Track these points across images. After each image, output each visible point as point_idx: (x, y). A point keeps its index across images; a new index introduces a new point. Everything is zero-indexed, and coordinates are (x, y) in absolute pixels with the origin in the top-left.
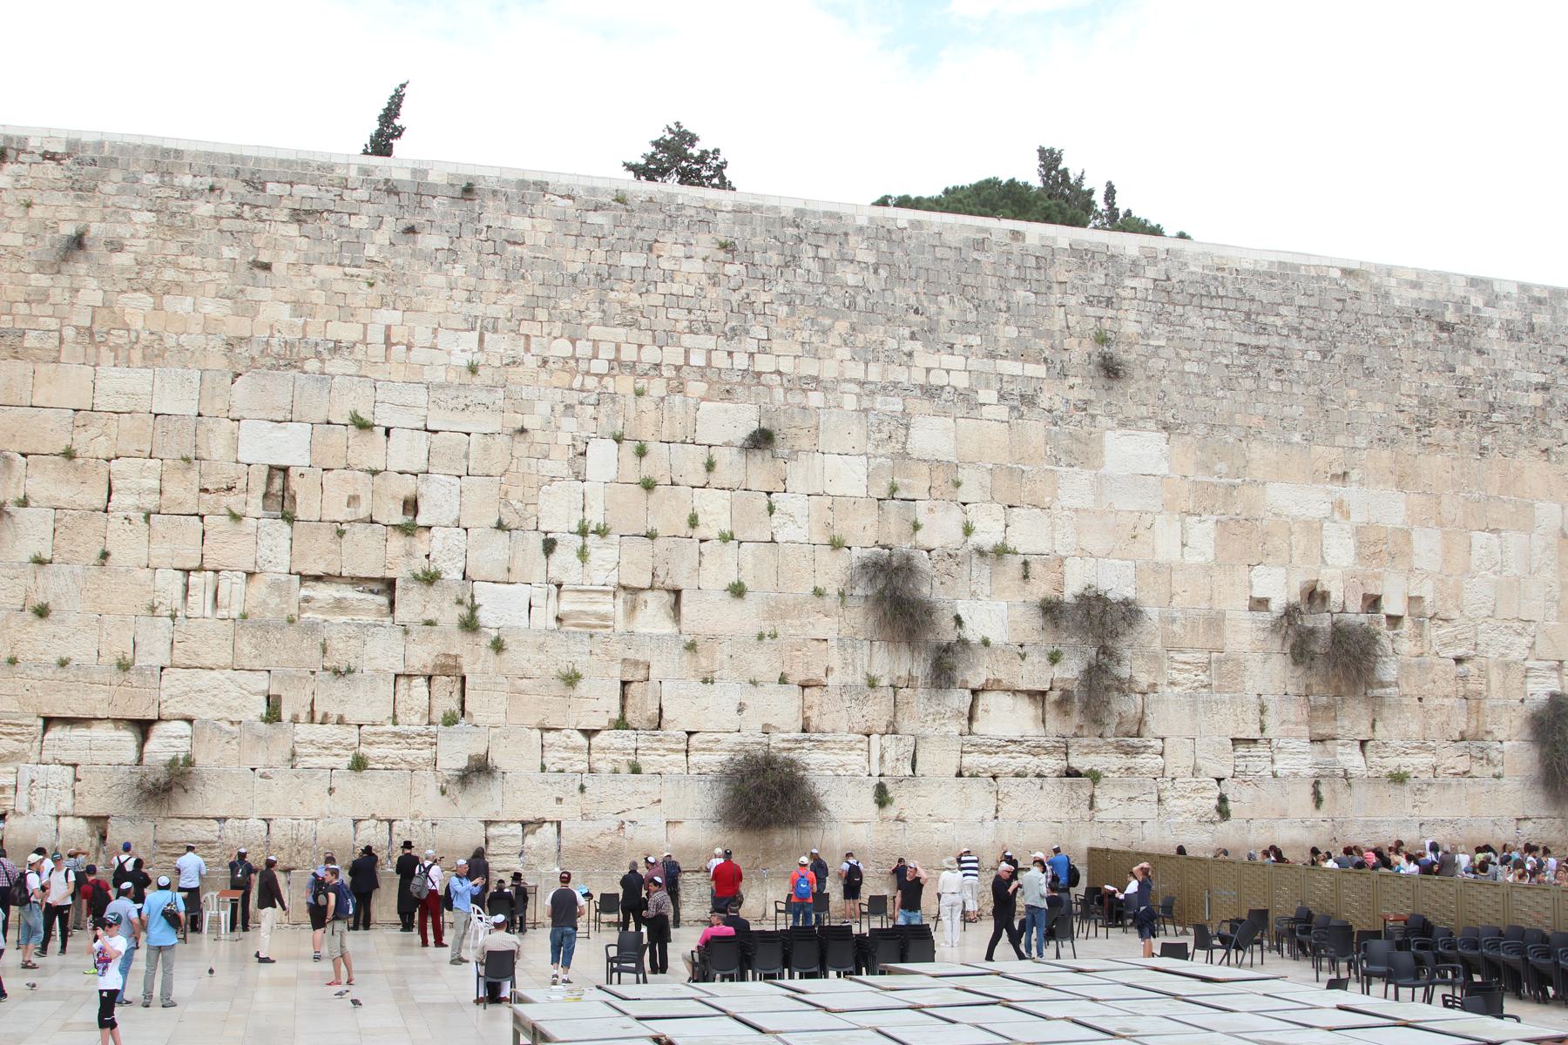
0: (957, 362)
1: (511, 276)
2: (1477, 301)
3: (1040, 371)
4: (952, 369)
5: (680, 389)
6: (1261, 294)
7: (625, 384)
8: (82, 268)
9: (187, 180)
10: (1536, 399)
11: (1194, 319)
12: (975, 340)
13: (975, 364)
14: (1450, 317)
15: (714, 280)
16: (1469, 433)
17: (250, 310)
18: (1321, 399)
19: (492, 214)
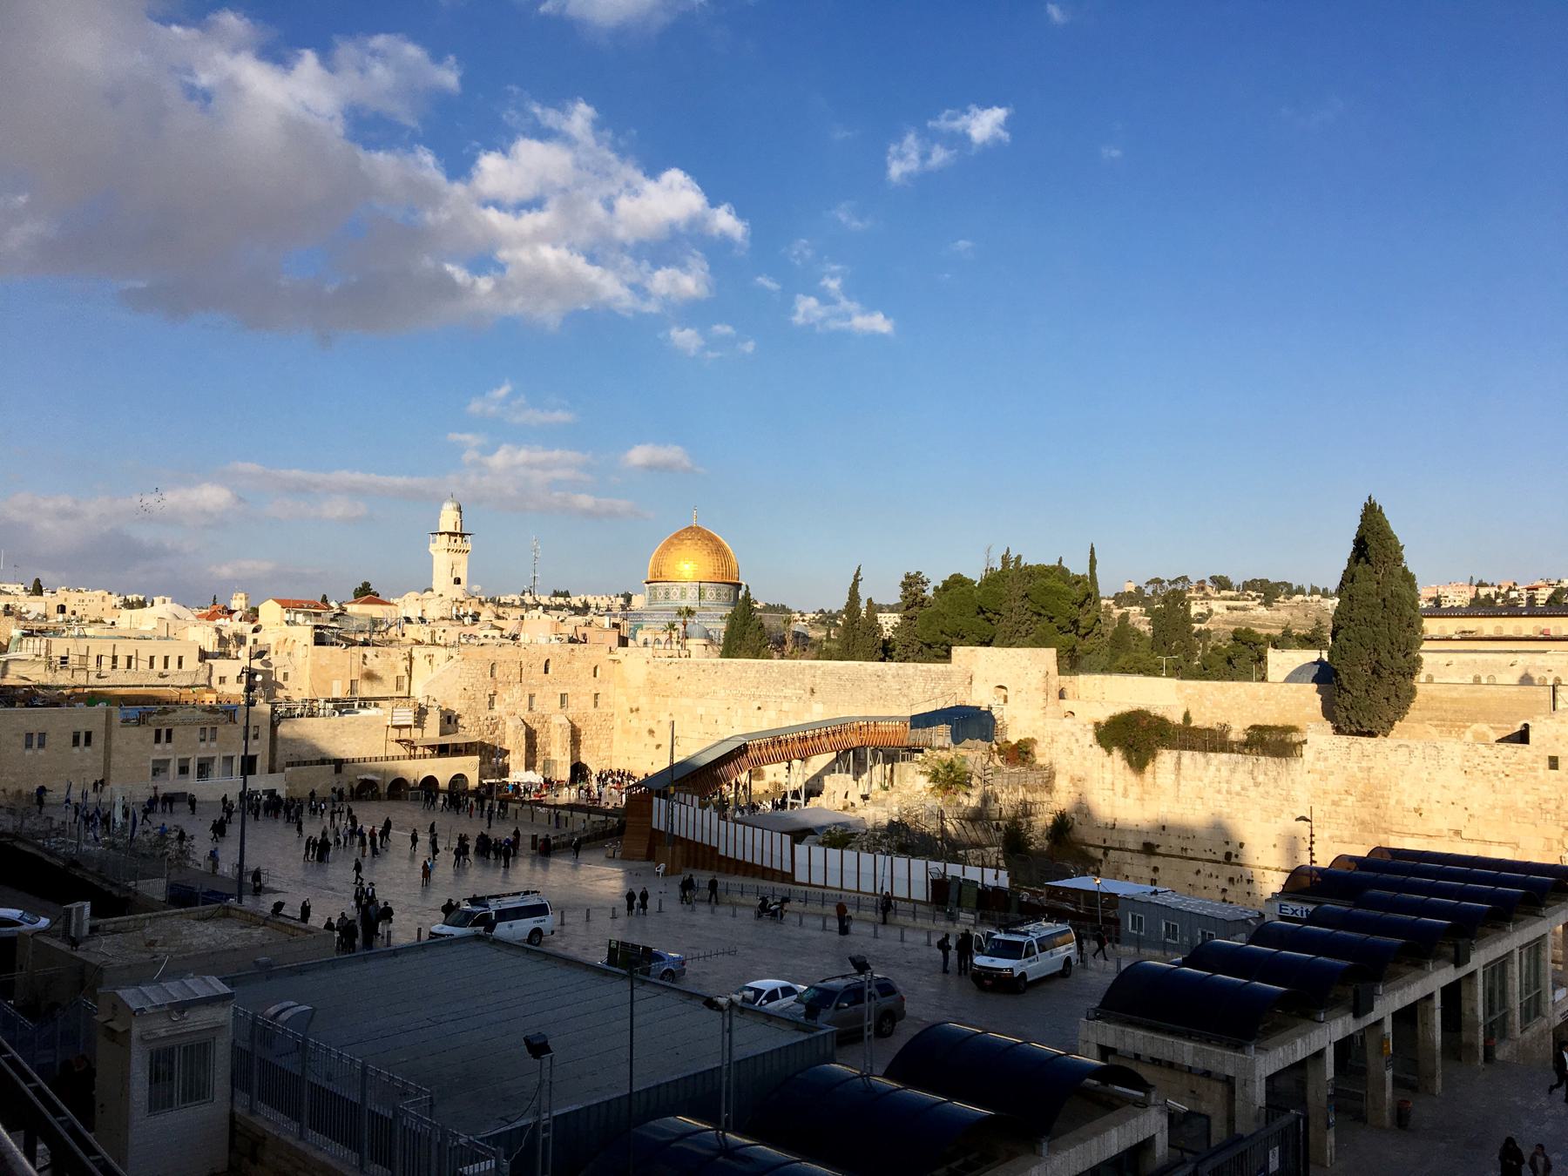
0: (789, 691)
1: (729, 679)
2: (886, 669)
3: (803, 692)
4: (788, 692)
5: (750, 698)
6: (842, 672)
7: (742, 698)
8: (679, 681)
9: (691, 666)
10: (898, 692)
11: (829, 678)
12: (793, 686)
13: (793, 691)
14: (880, 674)
15: (755, 677)
16: (882, 701)
17: (698, 688)
18: (852, 695)
19: (726, 667)
